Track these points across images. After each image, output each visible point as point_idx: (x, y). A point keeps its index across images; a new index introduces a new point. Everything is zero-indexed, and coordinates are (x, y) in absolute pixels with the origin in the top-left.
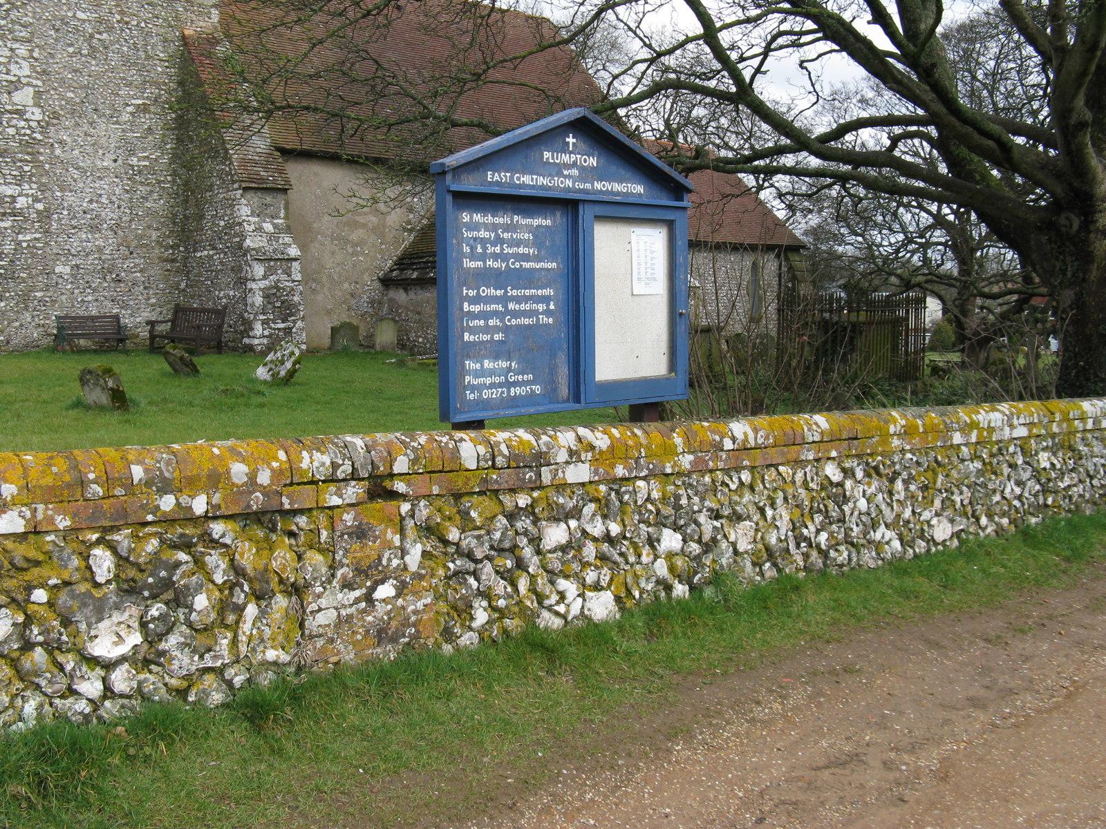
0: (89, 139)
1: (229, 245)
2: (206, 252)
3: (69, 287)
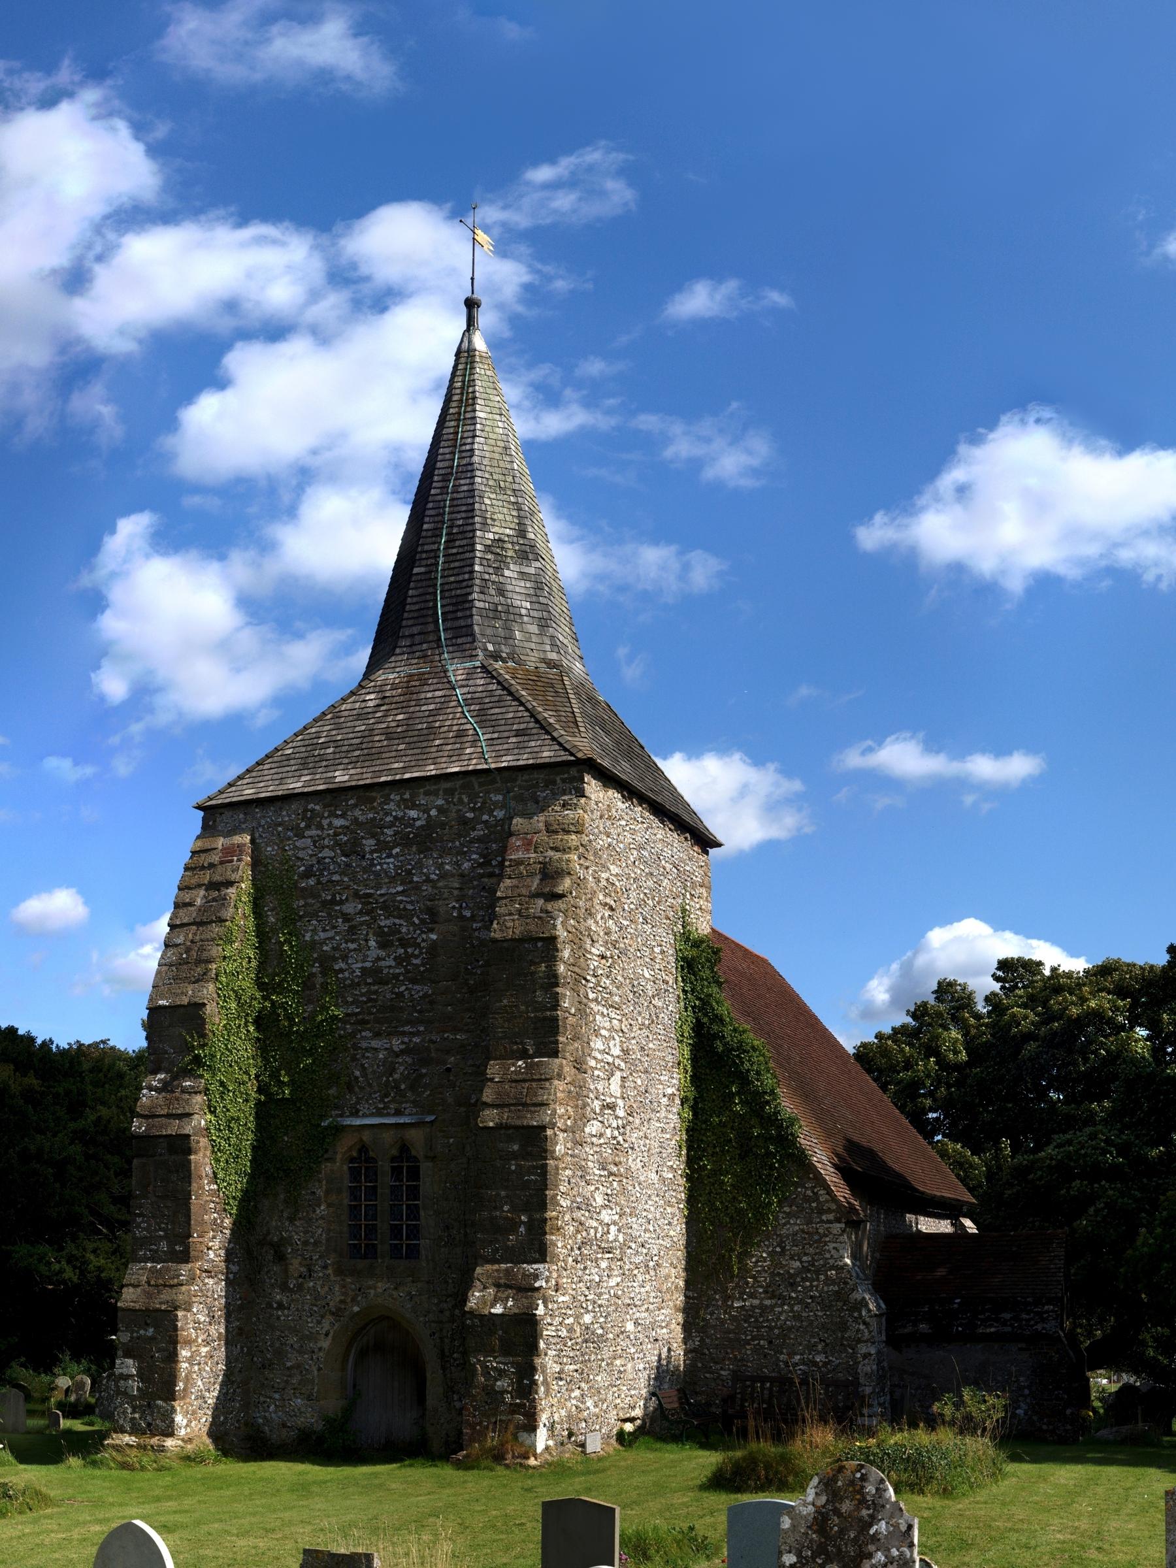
0: (647, 1142)
2: (756, 1302)
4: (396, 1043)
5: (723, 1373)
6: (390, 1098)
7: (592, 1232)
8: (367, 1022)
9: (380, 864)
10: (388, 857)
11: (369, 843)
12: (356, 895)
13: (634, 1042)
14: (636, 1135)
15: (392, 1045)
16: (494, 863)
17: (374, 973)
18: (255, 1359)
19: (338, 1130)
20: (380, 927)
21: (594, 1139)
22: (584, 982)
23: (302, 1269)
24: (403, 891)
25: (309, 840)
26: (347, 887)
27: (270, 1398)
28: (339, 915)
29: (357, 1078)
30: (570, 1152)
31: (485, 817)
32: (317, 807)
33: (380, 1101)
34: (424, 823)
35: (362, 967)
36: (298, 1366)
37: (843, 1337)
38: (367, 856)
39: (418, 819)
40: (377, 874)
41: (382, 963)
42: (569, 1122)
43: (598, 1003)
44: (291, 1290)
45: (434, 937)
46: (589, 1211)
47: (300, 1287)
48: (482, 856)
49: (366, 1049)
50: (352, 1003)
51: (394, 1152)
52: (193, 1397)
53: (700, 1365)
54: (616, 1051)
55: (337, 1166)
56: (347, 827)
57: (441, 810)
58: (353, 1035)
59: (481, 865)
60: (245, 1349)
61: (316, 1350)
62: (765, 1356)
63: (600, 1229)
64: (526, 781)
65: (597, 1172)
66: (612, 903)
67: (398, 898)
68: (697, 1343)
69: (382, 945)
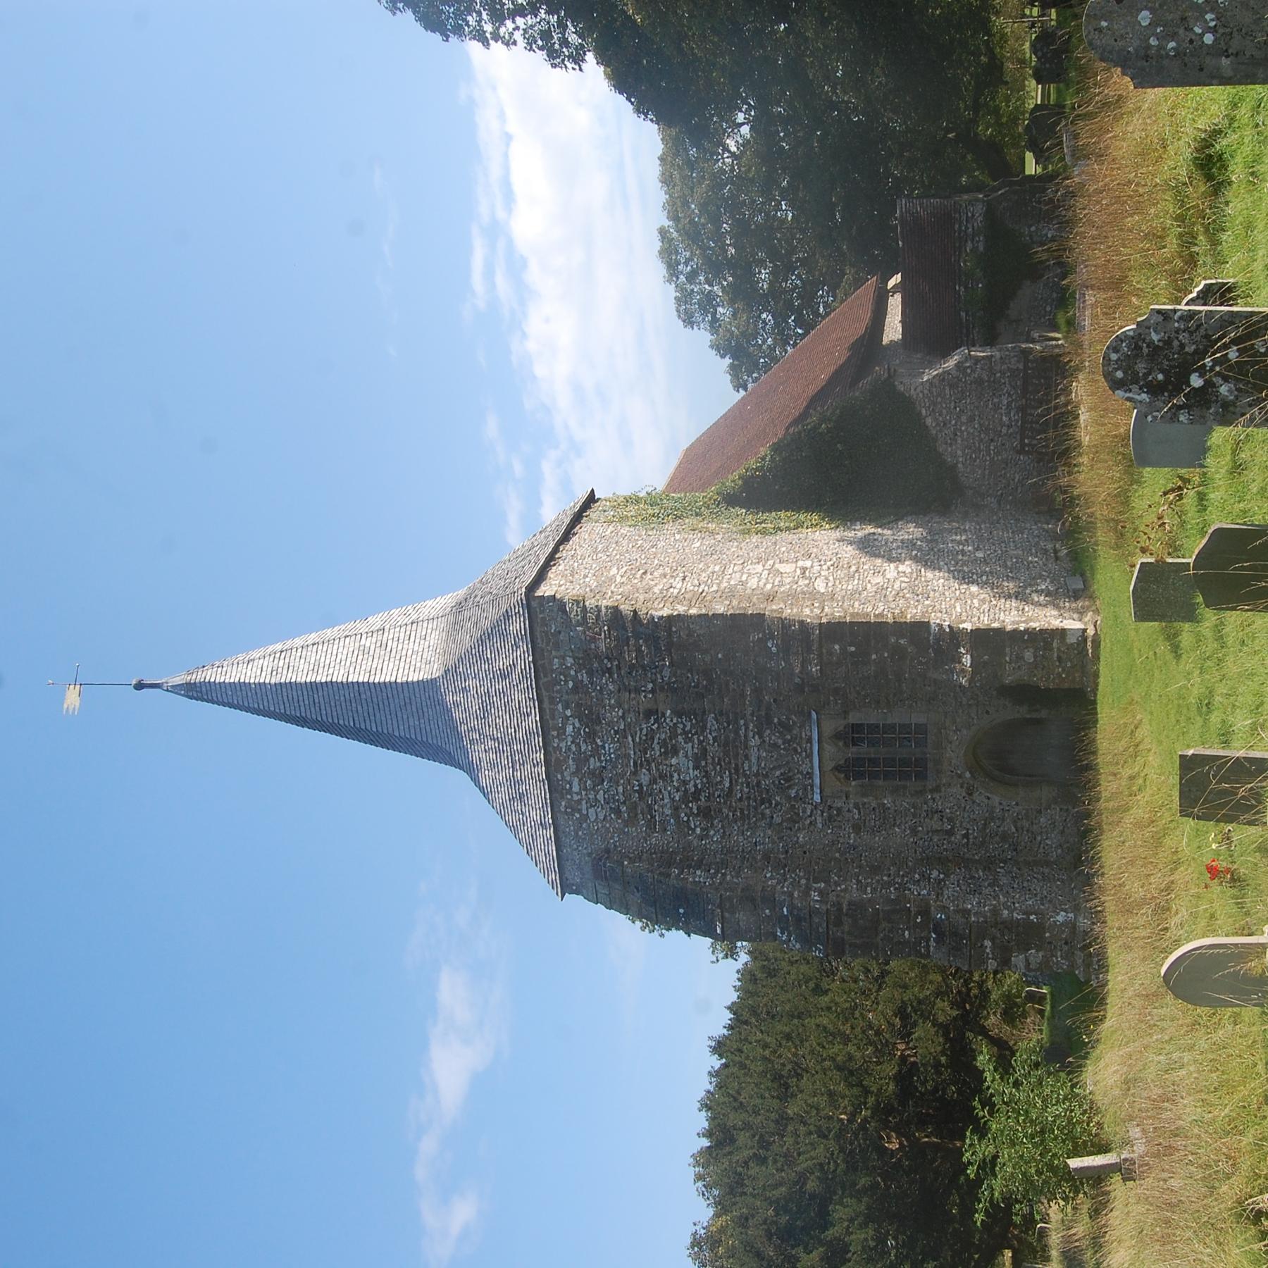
0: (831, 542)
1: (953, 404)
3: (1000, 552)
4: (754, 742)
5: (1016, 480)
6: (799, 748)
7: (903, 585)
8: (736, 765)
9: (610, 755)
10: (604, 748)
11: (593, 763)
12: (635, 773)
13: (751, 554)
14: (826, 551)
15: (755, 746)
16: (609, 666)
17: (699, 759)
18: (1009, 857)
20: (661, 755)
21: (830, 584)
22: (704, 594)
23: (935, 819)
24: (632, 737)
25: (590, 810)
26: (629, 781)
27: (1040, 843)
28: (650, 787)
29: (782, 774)
30: (840, 604)
31: (572, 673)
32: (563, 803)
33: (800, 755)
34: (577, 720)
35: (693, 769)
36: (1015, 822)
37: (989, 381)
38: (603, 764)
39: (574, 724)
40: (618, 757)
41: (690, 753)
42: (816, 605)
43: (721, 582)
44: (953, 828)
45: (669, 712)
46: (887, 588)
47: (950, 820)
48: (603, 675)
49: (759, 766)
50: (722, 777)
51: (841, 744)
52: (1042, 907)
53: (1011, 498)
54: (759, 568)
56: (580, 780)
57: (566, 707)
58: (745, 775)
59: (611, 676)
60: (1002, 865)
61: (1002, 807)
62: (1003, 445)
63: (902, 579)
64: (543, 641)
65: (856, 582)
66: (642, 571)
67: (638, 740)
68: (993, 500)
69: (675, 752)
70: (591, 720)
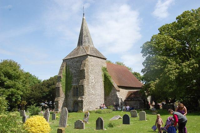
19: (72, 86)
55: (72, 89)
70: (77, 62)
